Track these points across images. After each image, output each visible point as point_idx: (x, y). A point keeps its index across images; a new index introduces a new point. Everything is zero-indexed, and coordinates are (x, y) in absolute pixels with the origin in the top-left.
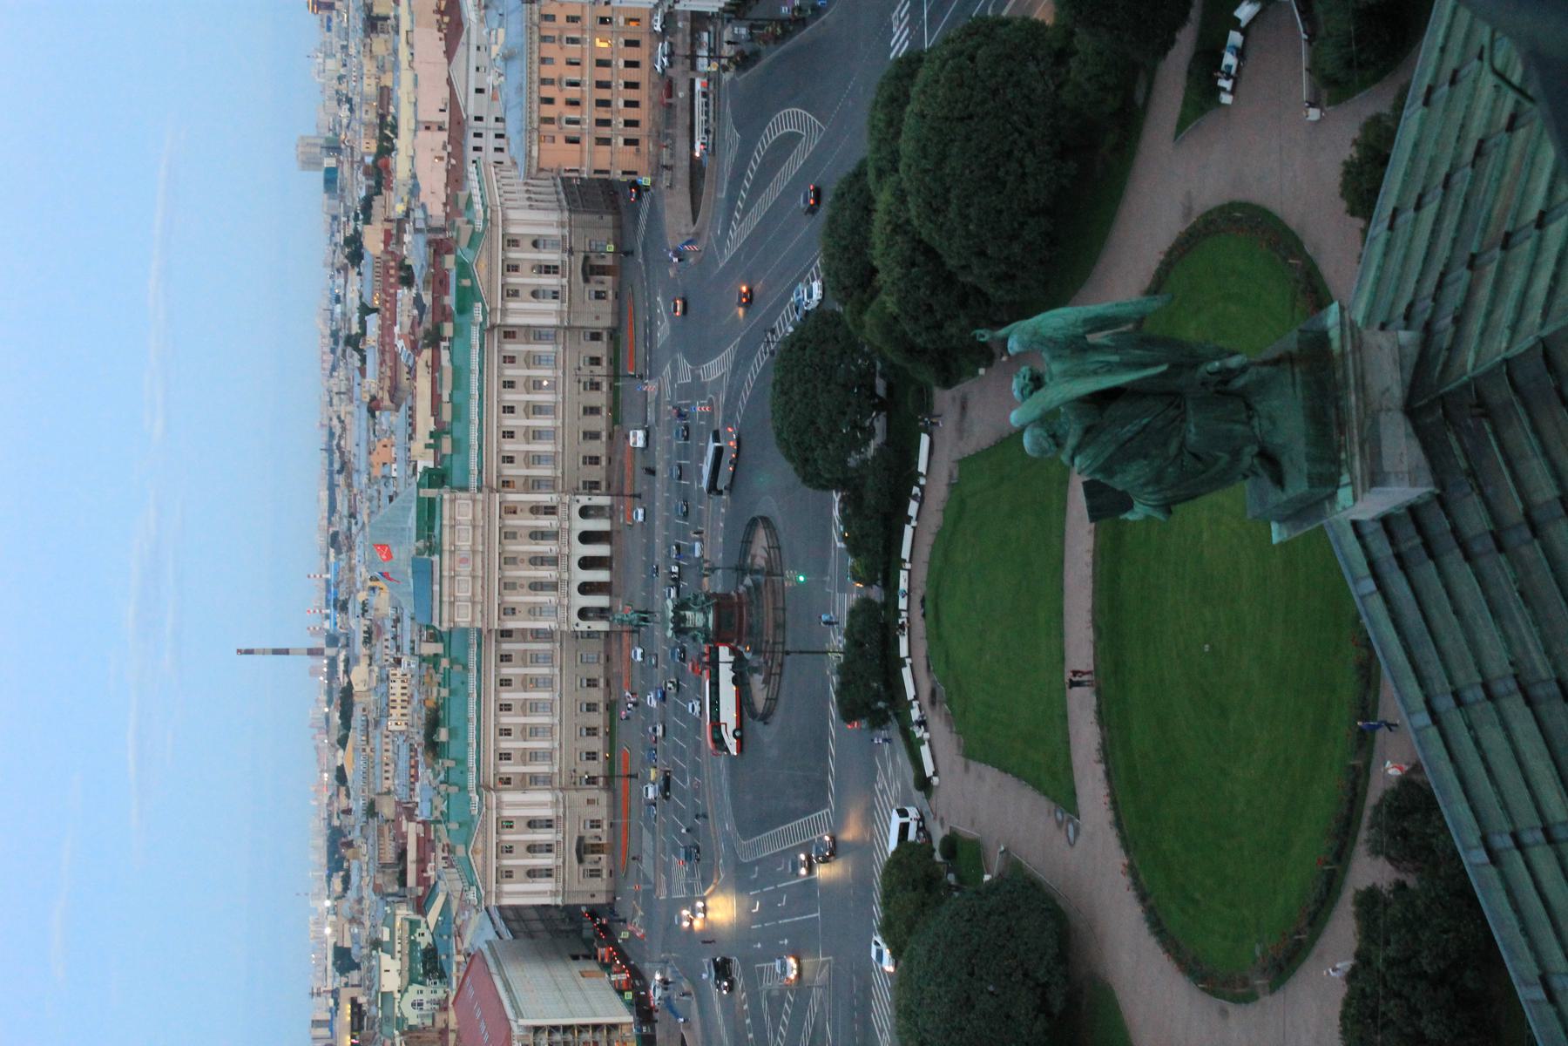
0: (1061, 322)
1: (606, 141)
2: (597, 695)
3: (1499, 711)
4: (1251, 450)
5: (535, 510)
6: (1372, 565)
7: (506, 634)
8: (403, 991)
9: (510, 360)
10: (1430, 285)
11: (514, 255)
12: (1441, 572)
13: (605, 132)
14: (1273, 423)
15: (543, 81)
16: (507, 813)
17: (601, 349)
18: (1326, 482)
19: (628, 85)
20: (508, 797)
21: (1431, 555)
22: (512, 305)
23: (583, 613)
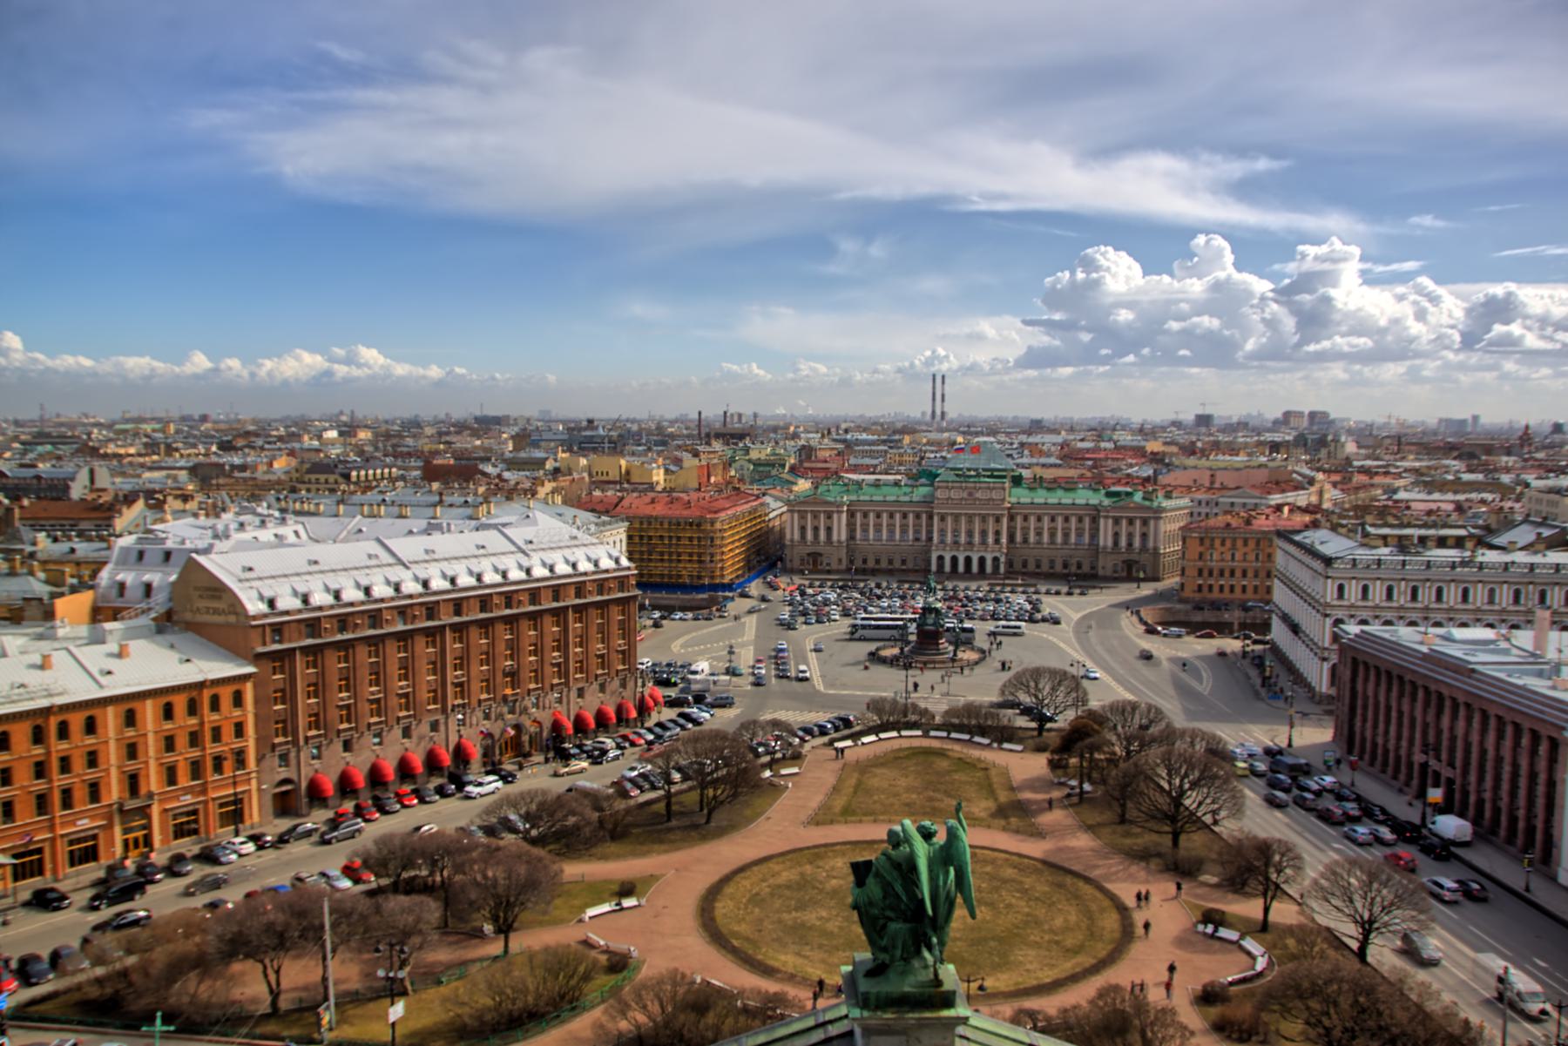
2: (897, 564)
4: (884, 957)
5: (997, 533)
6: (831, 1022)
7: (930, 517)
8: (750, 461)
9: (1080, 520)
11: (1138, 523)
13: (1206, 573)
16: (835, 516)
17: (1086, 569)
18: (864, 1002)
22: (1110, 521)
23: (941, 558)
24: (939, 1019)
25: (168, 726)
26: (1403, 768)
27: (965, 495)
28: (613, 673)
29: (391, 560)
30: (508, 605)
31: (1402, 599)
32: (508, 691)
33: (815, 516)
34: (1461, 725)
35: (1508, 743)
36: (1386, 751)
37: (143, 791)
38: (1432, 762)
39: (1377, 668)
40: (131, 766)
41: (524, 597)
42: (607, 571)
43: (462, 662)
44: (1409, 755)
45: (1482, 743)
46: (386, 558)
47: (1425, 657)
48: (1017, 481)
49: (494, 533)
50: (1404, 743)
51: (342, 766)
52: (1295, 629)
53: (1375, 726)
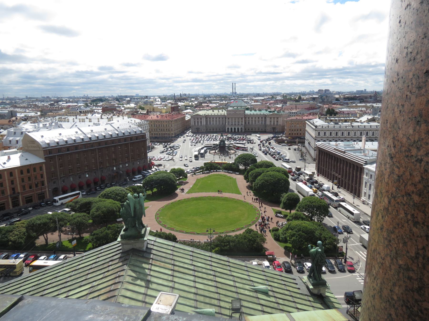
1: (290, 130)
9: (262, 118)
17: (263, 130)
20: (205, 119)
23: (228, 128)
25: (22, 176)
29: (81, 133)
31: (334, 135)
37: (16, 192)
40: (13, 186)
47: (335, 149)
48: (247, 109)
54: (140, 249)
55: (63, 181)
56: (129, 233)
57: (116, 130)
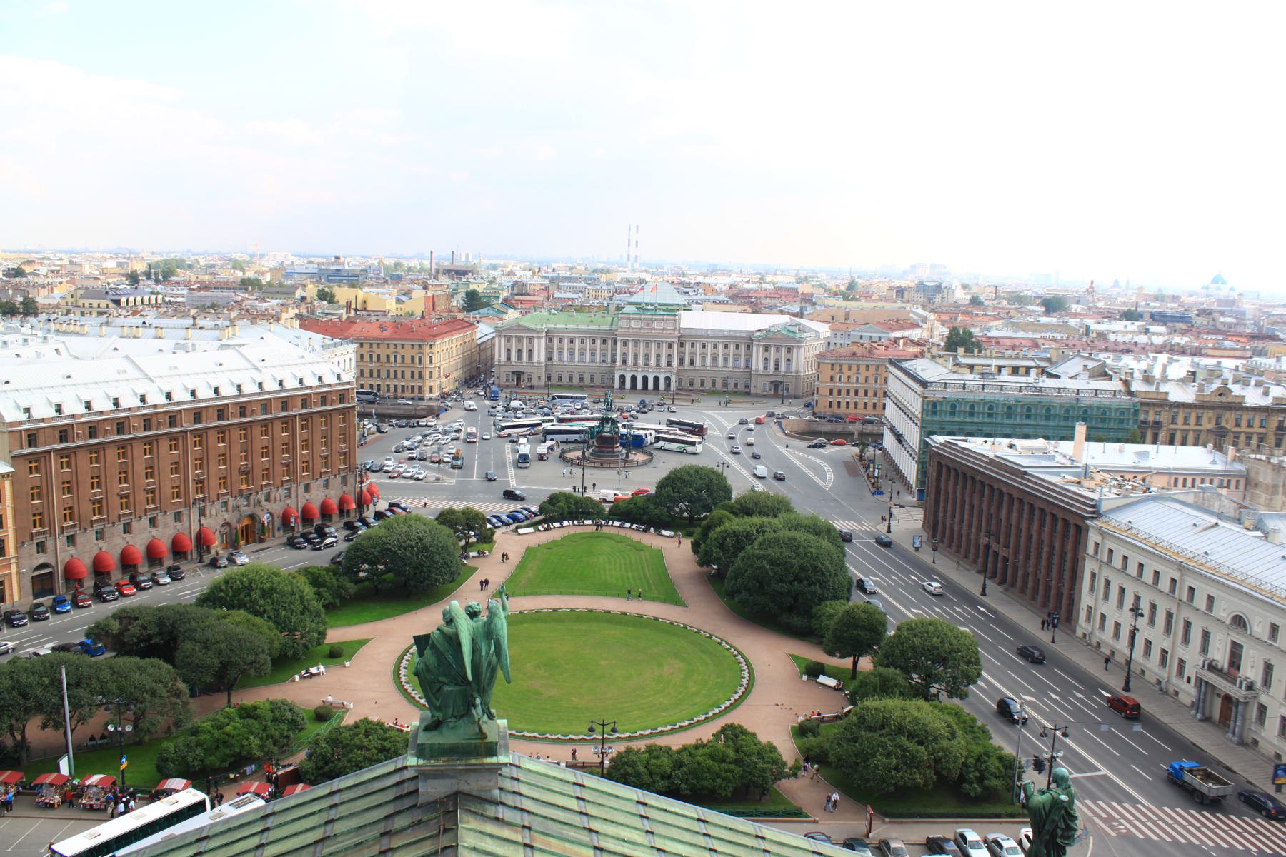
0: (499, 626)
1: (831, 393)
3: (320, 826)
4: (439, 715)
7: (615, 342)
10: (527, 804)
12: (387, 802)
13: (835, 392)
14: (453, 728)
15: (858, 366)
19: (856, 404)
20: (543, 341)
21: (396, 799)
23: (623, 377)
24: (483, 764)
26: (972, 550)
27: (643, 325)
28: (336, 471)
29: (139, 375)
30: (243, 414)
32: (244, 487)
33: (519, 339)
34: (1015, 514)
35: (1047, 529)
36: (960, 536)
38: (994, 545)
39: (956, 470)
41: (257, 408)
42: (330, 385)
43: (201, 462)
44: (977, 540)
45: (1029, 529)
46: (133, 373)
47: (991, 462)
49: (230, 352)
50: (973, 530)
51: (95, 552)
52: (899, 438)
53: (953, 516)
54: (483, 795)
55: (71, 540)
56: (446, 738)
57: (257, 369)
